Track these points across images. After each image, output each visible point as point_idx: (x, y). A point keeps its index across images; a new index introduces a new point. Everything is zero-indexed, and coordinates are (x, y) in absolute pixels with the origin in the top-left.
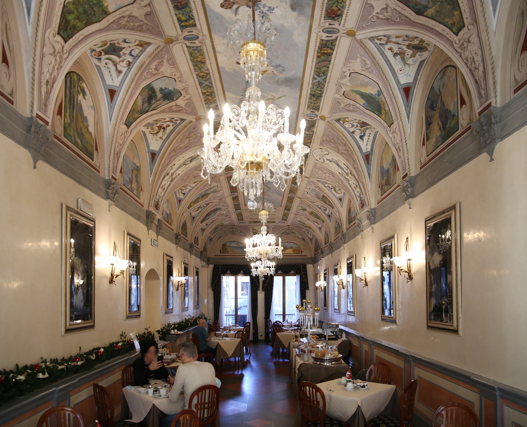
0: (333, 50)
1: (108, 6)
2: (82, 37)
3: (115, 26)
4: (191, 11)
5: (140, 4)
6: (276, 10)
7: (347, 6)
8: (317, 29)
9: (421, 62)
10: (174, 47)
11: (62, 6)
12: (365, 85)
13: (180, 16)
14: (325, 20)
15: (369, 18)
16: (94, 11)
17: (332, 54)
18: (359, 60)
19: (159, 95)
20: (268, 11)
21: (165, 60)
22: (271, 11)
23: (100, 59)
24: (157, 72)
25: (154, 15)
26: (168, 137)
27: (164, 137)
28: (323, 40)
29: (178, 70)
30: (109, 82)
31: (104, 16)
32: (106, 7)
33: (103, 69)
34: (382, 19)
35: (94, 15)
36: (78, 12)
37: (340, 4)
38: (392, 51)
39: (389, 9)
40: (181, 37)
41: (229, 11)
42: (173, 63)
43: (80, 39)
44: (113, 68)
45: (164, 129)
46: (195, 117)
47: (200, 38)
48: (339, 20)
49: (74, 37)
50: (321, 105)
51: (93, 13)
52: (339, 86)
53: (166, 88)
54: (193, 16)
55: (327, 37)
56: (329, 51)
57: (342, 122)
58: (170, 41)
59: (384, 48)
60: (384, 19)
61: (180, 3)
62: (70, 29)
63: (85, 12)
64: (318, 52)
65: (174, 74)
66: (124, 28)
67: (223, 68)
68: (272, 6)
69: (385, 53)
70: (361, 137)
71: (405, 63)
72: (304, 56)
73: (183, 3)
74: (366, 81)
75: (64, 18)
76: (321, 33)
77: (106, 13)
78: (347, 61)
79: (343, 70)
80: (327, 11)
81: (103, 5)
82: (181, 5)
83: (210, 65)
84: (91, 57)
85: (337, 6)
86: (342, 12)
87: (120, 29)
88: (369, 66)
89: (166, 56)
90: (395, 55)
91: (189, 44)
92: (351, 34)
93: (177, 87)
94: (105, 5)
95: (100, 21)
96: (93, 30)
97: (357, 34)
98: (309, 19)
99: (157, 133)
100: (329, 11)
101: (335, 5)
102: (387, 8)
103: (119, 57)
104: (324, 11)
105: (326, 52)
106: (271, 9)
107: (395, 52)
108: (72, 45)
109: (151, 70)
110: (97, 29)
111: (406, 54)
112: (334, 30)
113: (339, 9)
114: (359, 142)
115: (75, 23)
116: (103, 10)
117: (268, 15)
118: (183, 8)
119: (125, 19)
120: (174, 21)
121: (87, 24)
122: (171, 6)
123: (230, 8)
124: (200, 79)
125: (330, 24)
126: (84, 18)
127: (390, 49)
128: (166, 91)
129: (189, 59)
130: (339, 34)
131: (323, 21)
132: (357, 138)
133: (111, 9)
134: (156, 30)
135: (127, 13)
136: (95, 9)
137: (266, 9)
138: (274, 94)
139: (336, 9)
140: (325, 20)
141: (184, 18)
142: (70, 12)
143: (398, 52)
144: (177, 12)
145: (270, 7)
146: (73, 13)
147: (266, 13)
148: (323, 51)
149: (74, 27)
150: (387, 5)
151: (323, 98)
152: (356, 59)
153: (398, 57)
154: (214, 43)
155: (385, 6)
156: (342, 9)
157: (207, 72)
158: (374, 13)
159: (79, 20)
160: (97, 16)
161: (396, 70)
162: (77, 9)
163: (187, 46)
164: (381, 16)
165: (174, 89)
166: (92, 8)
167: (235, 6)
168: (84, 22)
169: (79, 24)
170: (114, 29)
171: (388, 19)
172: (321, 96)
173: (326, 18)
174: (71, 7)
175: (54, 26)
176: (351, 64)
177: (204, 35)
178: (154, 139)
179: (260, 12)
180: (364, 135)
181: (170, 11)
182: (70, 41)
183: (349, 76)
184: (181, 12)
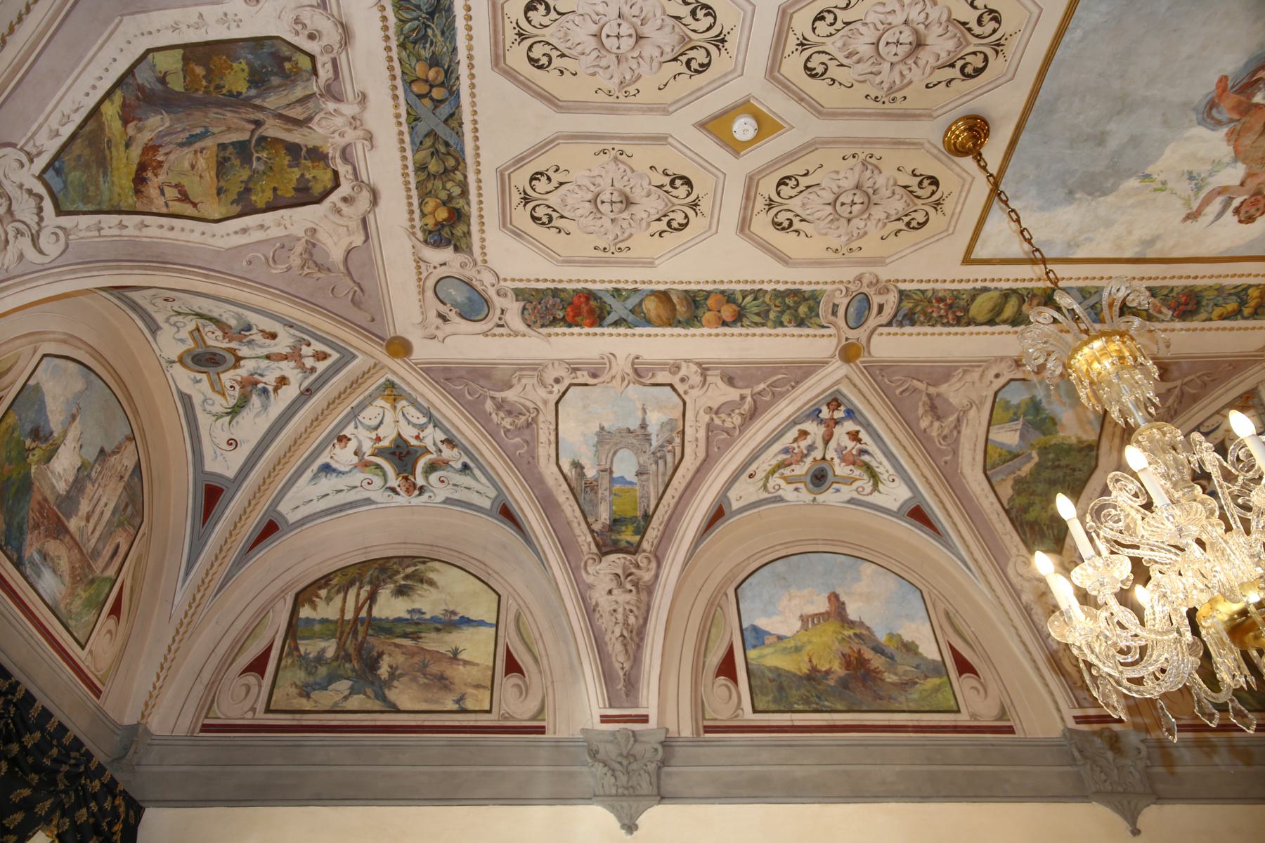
16: (1067, 466)
32: (1080, 441)
35: (1074, 470)
73: (1183, 300)
116: (1080, 450)
118: (1198, 303)
144: (1204, 315)
146: (1031, 504)
162: (1033, 493)
166: (1059, 466)
174: (1022, 500)
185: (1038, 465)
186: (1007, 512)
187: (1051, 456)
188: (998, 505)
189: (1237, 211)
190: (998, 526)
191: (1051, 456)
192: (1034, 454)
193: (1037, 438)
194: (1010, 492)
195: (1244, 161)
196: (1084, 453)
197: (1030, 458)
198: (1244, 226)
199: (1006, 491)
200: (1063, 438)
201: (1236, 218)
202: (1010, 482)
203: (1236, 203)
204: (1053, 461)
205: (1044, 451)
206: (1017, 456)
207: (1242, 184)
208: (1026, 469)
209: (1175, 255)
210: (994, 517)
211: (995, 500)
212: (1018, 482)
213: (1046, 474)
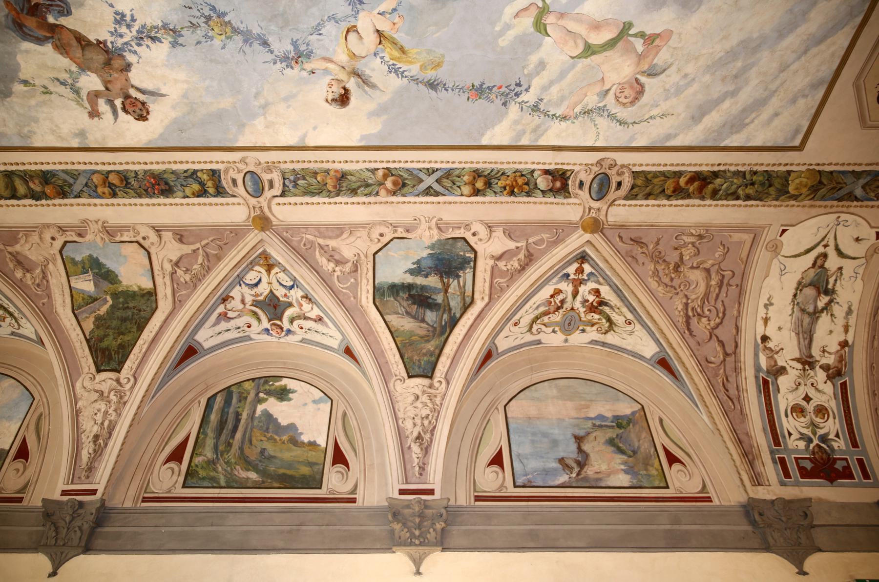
1: (139, 287)
2: (145, 347)
3: (184, 292)
4: (173, 172)
5: (152, 244)
6: (120, 8)
10: (281, 218)
11: (85, 343)
13: (188, 191)
16: (134, 308)
19: (433, 281)
20: (129, 26)
21: (321, 241)
22: (128, 18)
23: (289, 332)
24: (350, 264)
25: (186, 230)
26: (632, 310)
27: (630, 316)
29: (367, 226)
30: (335, 344)
31: (153, 298)
32: (140, 289)
33: (308, 336)
35: (140, 310)
36: (114, 329)
40: (253, 201)
41: (152, 107)
42: (338, 230)
43: (144, 350)
44: (307, 324)
45: (602, 303)
46: (580, 231)
47: (251, 168)
49: (132, 356)
51: (135, 311)
53: (418, 262)
54: (186, 171)
58: (263, 222)
61: (153, 185)
62: (117, 353)
63: (124, 320)
65: (375, 235)
66: (200, 280)
67: (363, 138)
68: (109, 16)
75: (96, 351)
77: (151, 295)
81: (134, 292)
82: (159, 184)
83: (356, 163)
84: (281, 340)
87: (195, 286)
89: (308, 236)
91: (277, 190)
93: (428, 242)
94: (136, 289)
95: (157, 307)
96: (158, 325)
99: (609, 320)
103: (290, 305)
106: (120, 19)
108: (134, 367)
109: (338, 273)
110: (163, 318)
115: (119, 341)
116: (143, 296)
117: (144, 26)
118: (167, 183)
119: (180, 272)
120: (205, 204)
121: (141, 328)
122: (162, 200)
123: (143, 104)
124: (405, 190)
126: (129, 326)
128: (429, 263)
129: (327, 200)
133: (147, 285)
134: (225, 237)
135: (168, 267)
136: (131, 305)
137: (123, 29)
138: (509, 11)
141: (196, 187)
142: (101, 340)
145: (117, 22)
146: (106, 336)
147: (138, 32)
149: (121, 346)
154: (268, 145)
157: (380, 173)
159: (123, 334)
160: (145, 307)
163: (283, 195)
165: (432, 247)
166: (128, 308)
167: (133, 93)
168: (135, 329)
169: (127, 338)
170: (188, 296)
174: (100, 332)
175: (86, 370)
177: (243, 161)
178: (625, 336)
179: (139, 45)
181: (177, 205)
182: (128, 364)
184: (179, 187)
185: (112, 306)
186: (88, 341)
187: (121, 300)
188: (82, 336)
189: (124, 109)
190: (80, 352)
191: (121, 300)
192: (108, 298)
193: (106, 286)
194: (92, 326)
195: (90, 69)
196: (146, 298)
197: (106, 301)
198: (141, 122)
199: (89, 325)
200: (126, 286)
201: (129, 118)
202: (92, 319)
203: (118, 103)
204: (123, 303)
205: (115, 295)
206: (96, 300)
207: (107, 89)
208: (104, 310)
209: (111, 145)
210: (78, 345)
211: (80, 332)
212: (98, 319)
213: (119, 314)
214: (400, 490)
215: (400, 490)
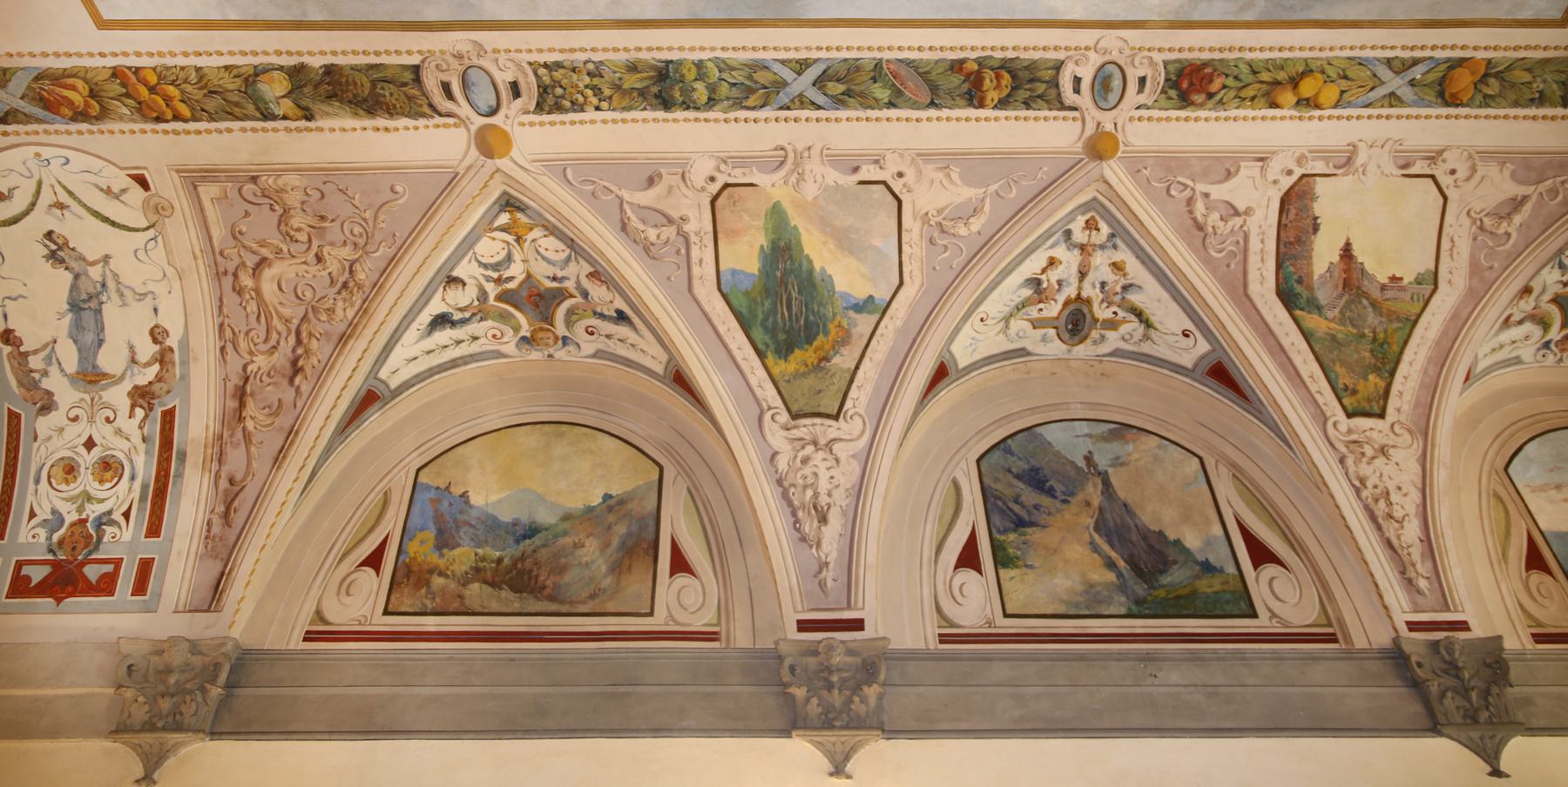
0: (1003, 104)
7: (1222, 114)
8: (1121, 44)
9: (1023, 349)
12: (845, 241)
14: (1166, 63)
15: (1180, 179)
17: (981, 105)
18: (968, 193)
28: (1058, 66)
34: (1191, 212)
37: (1232, 93)
38: (1044, 271)
39: (1238, 221)
48: (1163, 102)
50: (591, 114)
52: (780, 159)
55: (1077, 81)
56: (993, 95)
57: (504, 218)
59: (1052, 246)
60: (1195, 220)
64: (980, 62)
69: (1033, 257)
70: (441, 321)
71: (1006, 320)
72: (954, 16)
74: (877, 242)
76: (1095, 60)
78: (946, 160)
79: (889, 156)
80: (1205, 64)
85: (1224, 87)
86: (1201, 106)
88: (962, 231)
90: (1035, 283)
92: (1099, 147)
97: (1112, 162)
98: (1171, 17)
100: (1208, 70)
101: (1230, 82)
102: (1237, 213)
104: (1206, 56)
105: (987, 84)
107: (1043, 277)
111: (1041, 306)
112: (1113, 98)
113: (1210, 96)
114: (415, 325)
125: (1142, 81)
127: (1052, 262)
130: (1093, 114)
131: (1159, 58)
132: (436, 307)
139: (1214, 87)
140: (1166, 63)
143: (1045, 285)
148: (989, 76)
150: (1248, 212)
151: (661, 114)
152: (968, 182)
153: (1027, 292)
155: (1241, 208)
156: (1210, 104)
158: (1201, 187)
161: (982, 308)
164: (1200, 208)
171: (1200, 228)
172: (666, 104)
173: (1171, 68)
176: (940, 175)
180: (453, 324)
183: (861, 183)
214: (799, 622)
215: (799, 622)
